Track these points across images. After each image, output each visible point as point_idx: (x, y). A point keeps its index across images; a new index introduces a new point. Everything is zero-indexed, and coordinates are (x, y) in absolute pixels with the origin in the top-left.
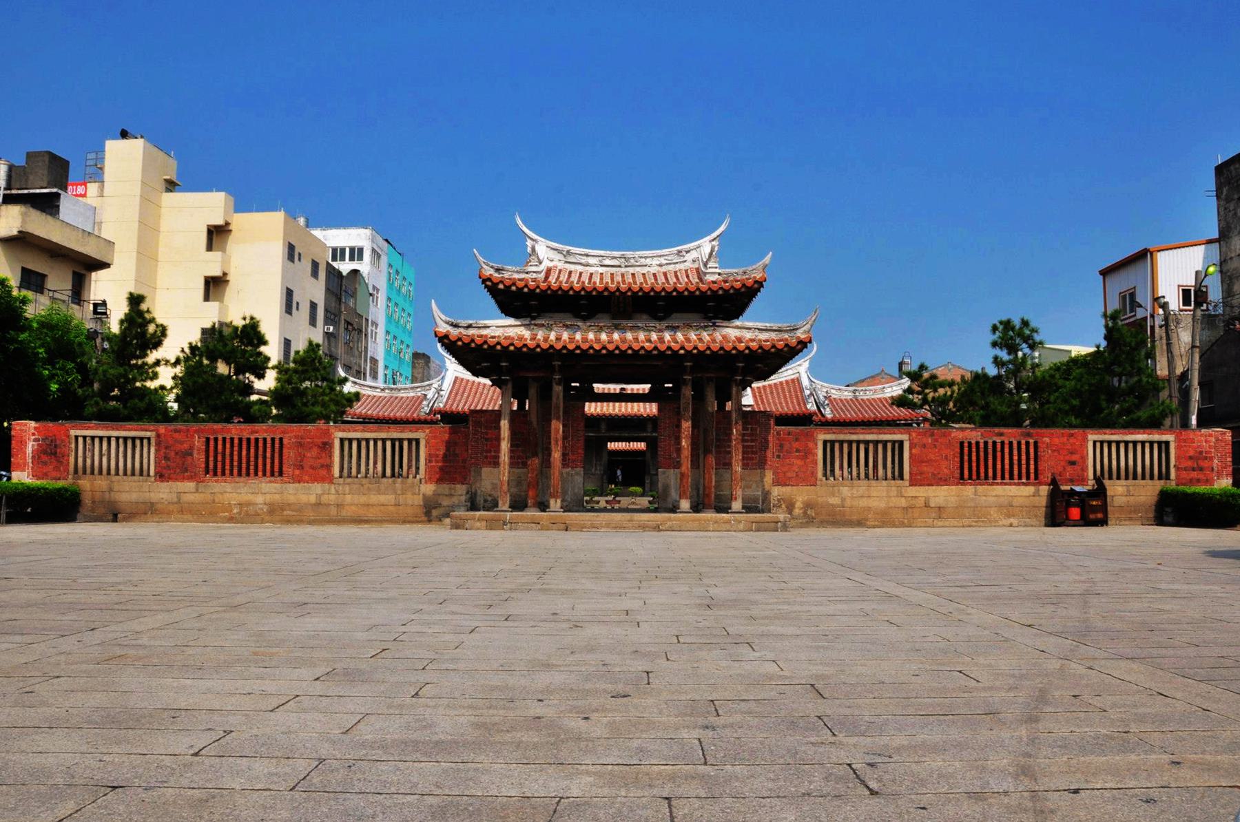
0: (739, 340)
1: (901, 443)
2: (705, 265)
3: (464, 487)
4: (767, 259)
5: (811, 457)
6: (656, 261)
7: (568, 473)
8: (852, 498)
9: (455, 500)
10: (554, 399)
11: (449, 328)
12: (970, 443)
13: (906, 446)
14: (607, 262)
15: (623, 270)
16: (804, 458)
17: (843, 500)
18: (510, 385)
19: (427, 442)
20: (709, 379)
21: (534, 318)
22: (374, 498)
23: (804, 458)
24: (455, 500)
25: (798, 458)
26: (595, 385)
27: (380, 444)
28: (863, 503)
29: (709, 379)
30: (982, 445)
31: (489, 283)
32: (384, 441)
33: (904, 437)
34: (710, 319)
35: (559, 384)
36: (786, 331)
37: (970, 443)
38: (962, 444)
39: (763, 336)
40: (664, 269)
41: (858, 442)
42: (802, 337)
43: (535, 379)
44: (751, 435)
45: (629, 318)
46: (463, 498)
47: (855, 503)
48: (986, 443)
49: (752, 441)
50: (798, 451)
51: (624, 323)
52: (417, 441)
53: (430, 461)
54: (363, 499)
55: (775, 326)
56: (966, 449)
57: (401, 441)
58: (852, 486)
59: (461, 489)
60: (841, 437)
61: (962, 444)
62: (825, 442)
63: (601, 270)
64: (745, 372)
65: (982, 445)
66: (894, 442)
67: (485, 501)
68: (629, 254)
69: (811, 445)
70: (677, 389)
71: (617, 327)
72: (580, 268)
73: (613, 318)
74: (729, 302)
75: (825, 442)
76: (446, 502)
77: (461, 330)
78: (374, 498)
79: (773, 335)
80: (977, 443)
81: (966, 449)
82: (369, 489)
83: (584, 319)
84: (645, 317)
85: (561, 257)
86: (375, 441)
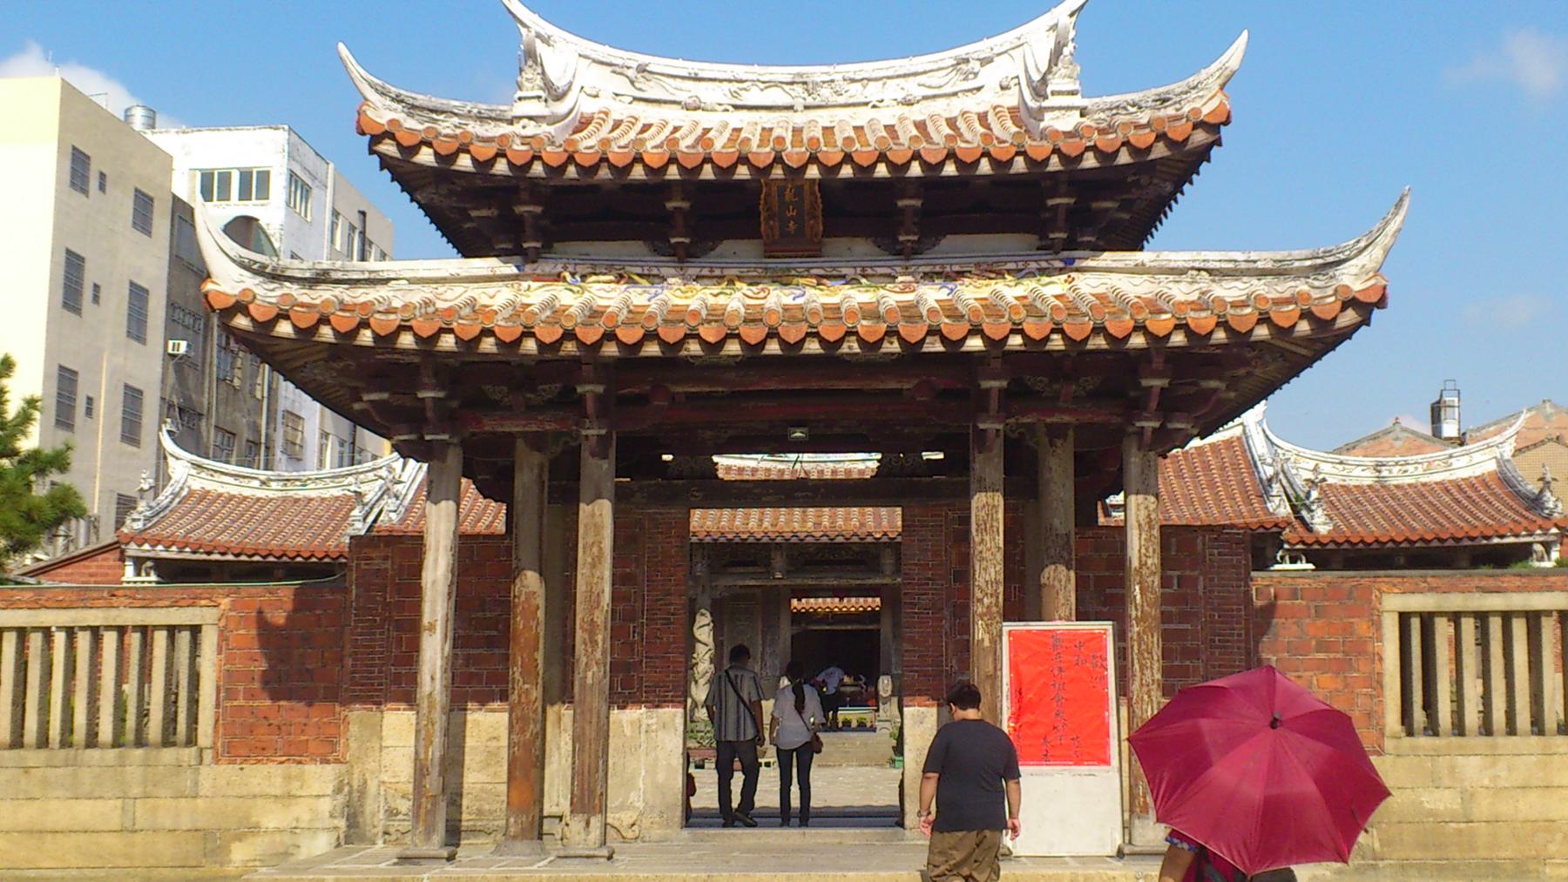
2: (1039, 90)
3: (330, 771)
4: (1234, 56)
5: (1363, 666)
6: (894, 90)
7: (637, 724)
8: (1497, 791)
9: (301, 812)
16: (1341, 667)
17: (1468, 796)
19: (223, 637)
20: (1056, 432)
22: (60, 811)
23: (1341, 667)
24: (301, 812)
25: (1321, 667)
26: (722, 461)
27: (83, 641)
28: (1529, 806)
29: (1056, 432)
31: (388, 148)
32: (96, 632)
36: (1304, 273)
39: (1230, 291)
40: (918, 113)
41: (1507, 617)
42: (1357, 286)
43: (537, 442)
46: (326, 805)
47: (1505, 808)
50: (1323, 646)
52: (195, 630)
53: (231, 694)
54: (27, 814)
55: (1265, 259)
57: (145, 631)
58: (1494, 755)
59: (319, 778)
60: (1455, 602)
62: (1404, 618)
64: (1170, 405)
67: (392, 813)
68: (817, 73)
69: (1362, 627)
70: (958, 464)
74: (1114, 196)
75: (1404, 618)
76: (272, 818)
77: (294, 290)
78: (60, 811)
79: (1260, 287)
82: (45, 783)
86: (70, 632)
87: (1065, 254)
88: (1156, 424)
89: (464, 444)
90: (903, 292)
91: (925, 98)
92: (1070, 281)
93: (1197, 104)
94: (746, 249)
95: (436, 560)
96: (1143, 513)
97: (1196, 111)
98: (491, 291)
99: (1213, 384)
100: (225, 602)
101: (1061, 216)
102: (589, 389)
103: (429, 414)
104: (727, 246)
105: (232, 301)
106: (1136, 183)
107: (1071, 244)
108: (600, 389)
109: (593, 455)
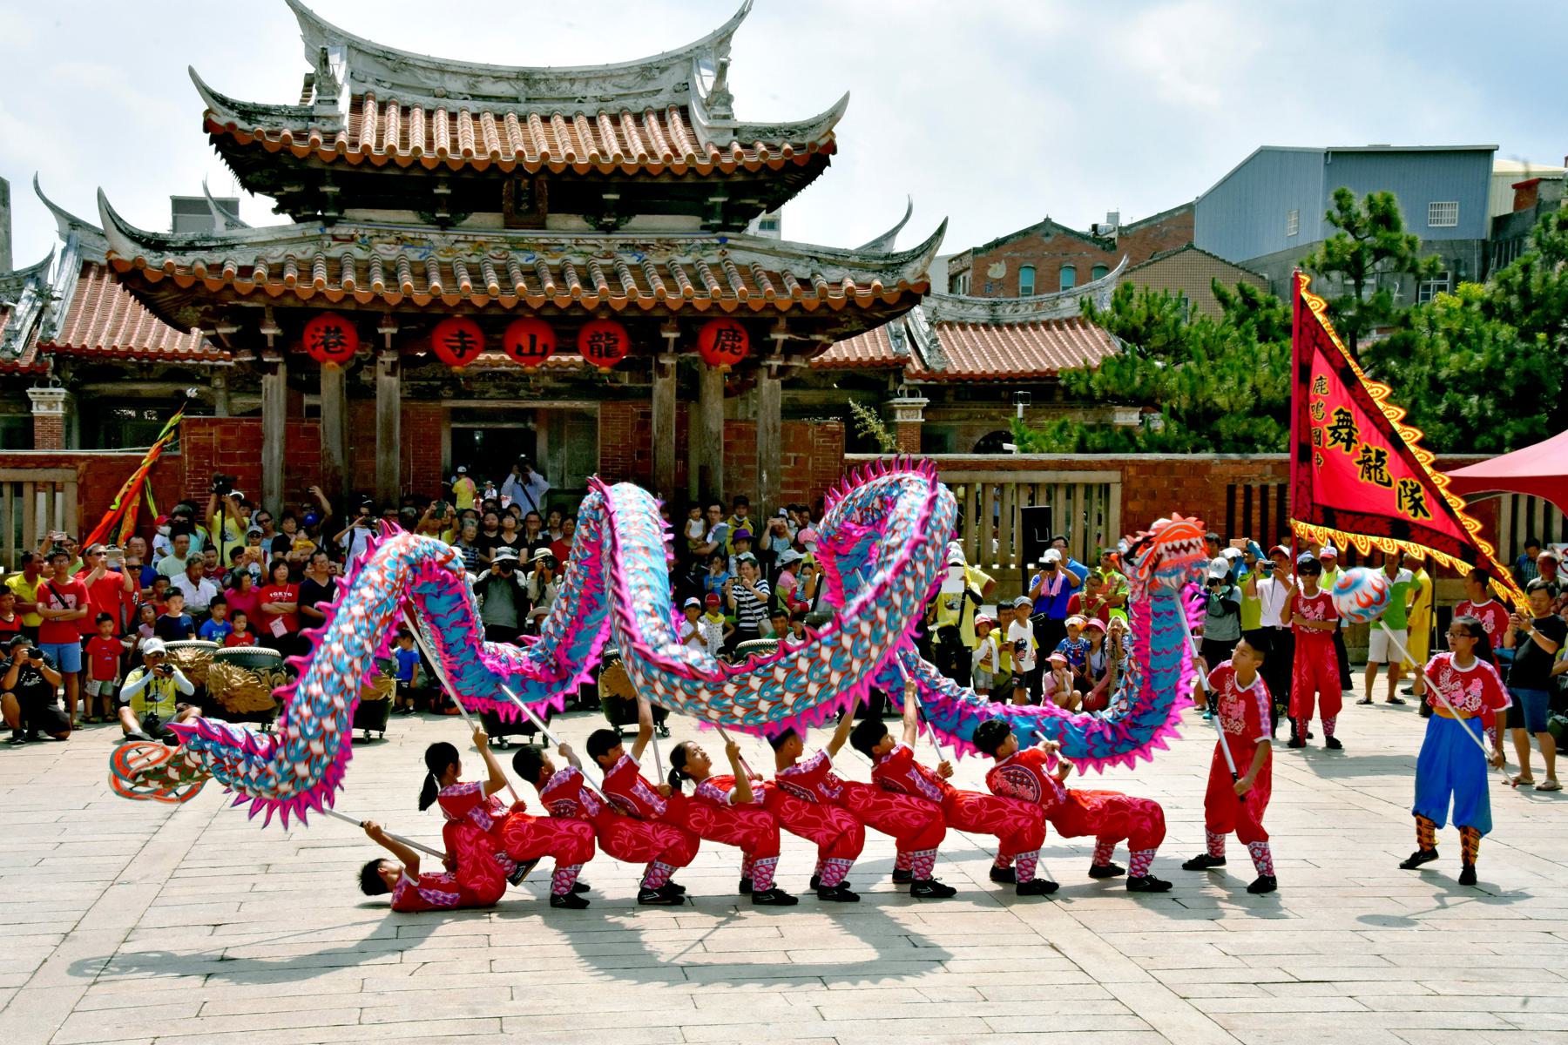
0: (777, 279)
1: (1105, 489)
10: (380, 405)
11: (141, 252)
12: (1248, 489)
13: (1116, 493)
14: (487, 88)
15: (522, 108)
18: (282, 370)
21: (330, 222)
30: (1273, 494)
33: (1113, 477)
34: (714, 229)
35: (391, 373)
37: (1248, 489)
38: (1231, 490)
42: (911, 280)
44: (795, 473)
45: (542, 226)
48: (1282, 489)
49: (797, 485)
51: (529, 235)
56: (1240, 502)
61: (1231, 490)
63: (475, 106)
65: (1273, 494)
66: (1088, 487)
71: (516, 245)
72: (430, 102)
73: (508, 225)
77: (171, 258)
80: (1264, 489)
81: (1240, 502)
83: (444, 225)
84: (576, 222)
85: (381, 72)
87: (720, 234)
88: (780, 363)
89: (286, 362)
90: (605, 258)
91: (619, 96)
92: (724, 253)
93: (814, 139)
94: (492, 219)
95: (272, 448)
96: (770, 421)
97: (813, 145)
98: (303, 248)
99: (818, 337)
100: (82, 466)
101: (718, 209)
102: (388, 331)
103: (271, 344)
104: (475, 219)
105: (130, 268)
106: (771, 189)
107: (725, 227)
108: (395, 331)
109: (387, 374)
